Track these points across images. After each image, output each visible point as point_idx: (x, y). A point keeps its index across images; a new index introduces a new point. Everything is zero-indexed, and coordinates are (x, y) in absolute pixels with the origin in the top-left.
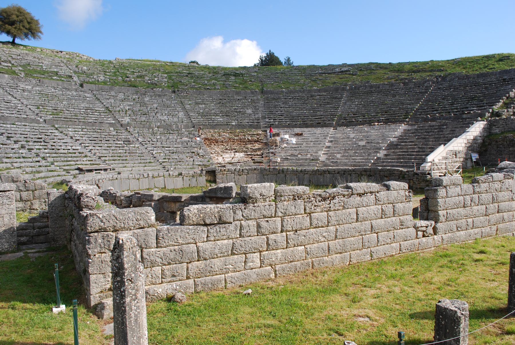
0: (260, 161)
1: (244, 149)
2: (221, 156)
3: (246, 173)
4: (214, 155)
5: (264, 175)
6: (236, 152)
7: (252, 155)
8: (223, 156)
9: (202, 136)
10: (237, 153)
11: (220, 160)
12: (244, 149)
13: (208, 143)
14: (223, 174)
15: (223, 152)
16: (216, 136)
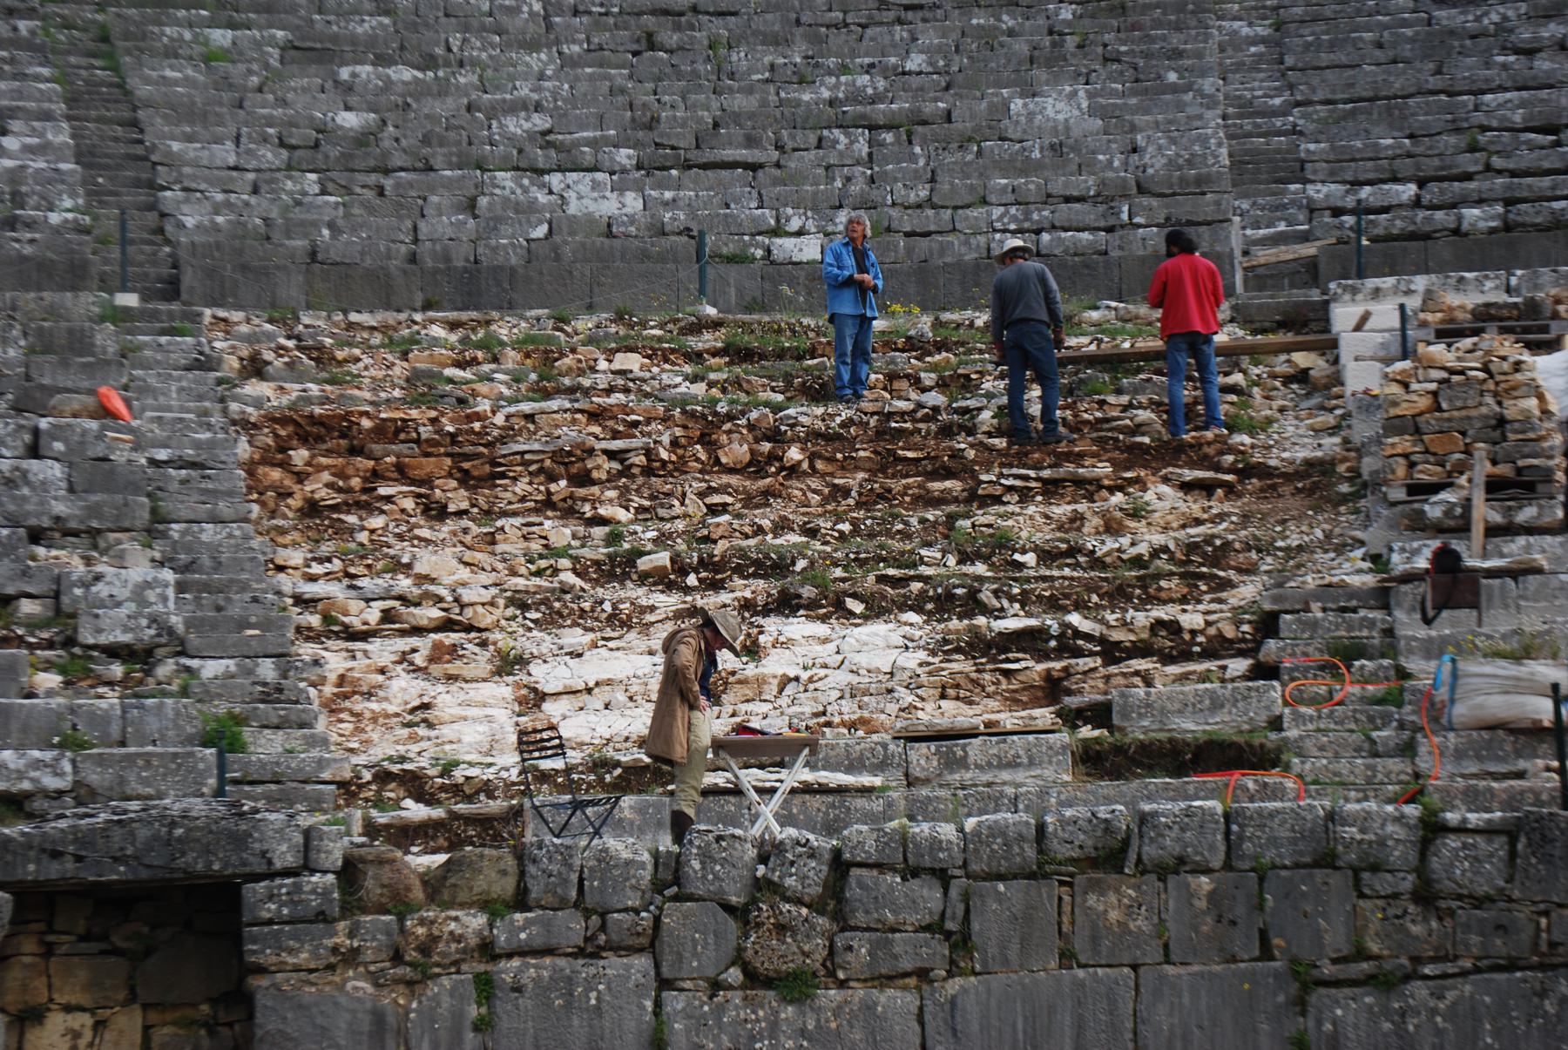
0: (1222, 724)
1: (938, 563)
2: (508, 664)
3: (909, 950)
4: (383, 650)
5: (1306, 984)
6: (786, 605)
7: (1069, 643)
8: (546, 675)
9: (254, 388)
10: (798, 627)
11: (475, 728)
12: (938, 563)
13: (317, 487)
14: (414, 964)
15: (552, 612)
16: (495, 396)
